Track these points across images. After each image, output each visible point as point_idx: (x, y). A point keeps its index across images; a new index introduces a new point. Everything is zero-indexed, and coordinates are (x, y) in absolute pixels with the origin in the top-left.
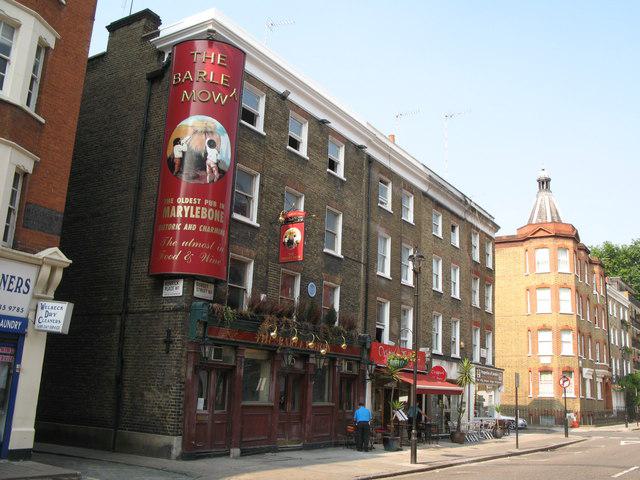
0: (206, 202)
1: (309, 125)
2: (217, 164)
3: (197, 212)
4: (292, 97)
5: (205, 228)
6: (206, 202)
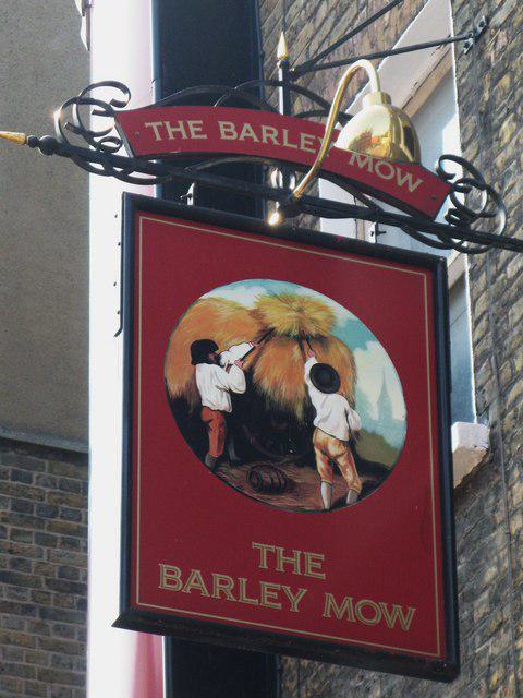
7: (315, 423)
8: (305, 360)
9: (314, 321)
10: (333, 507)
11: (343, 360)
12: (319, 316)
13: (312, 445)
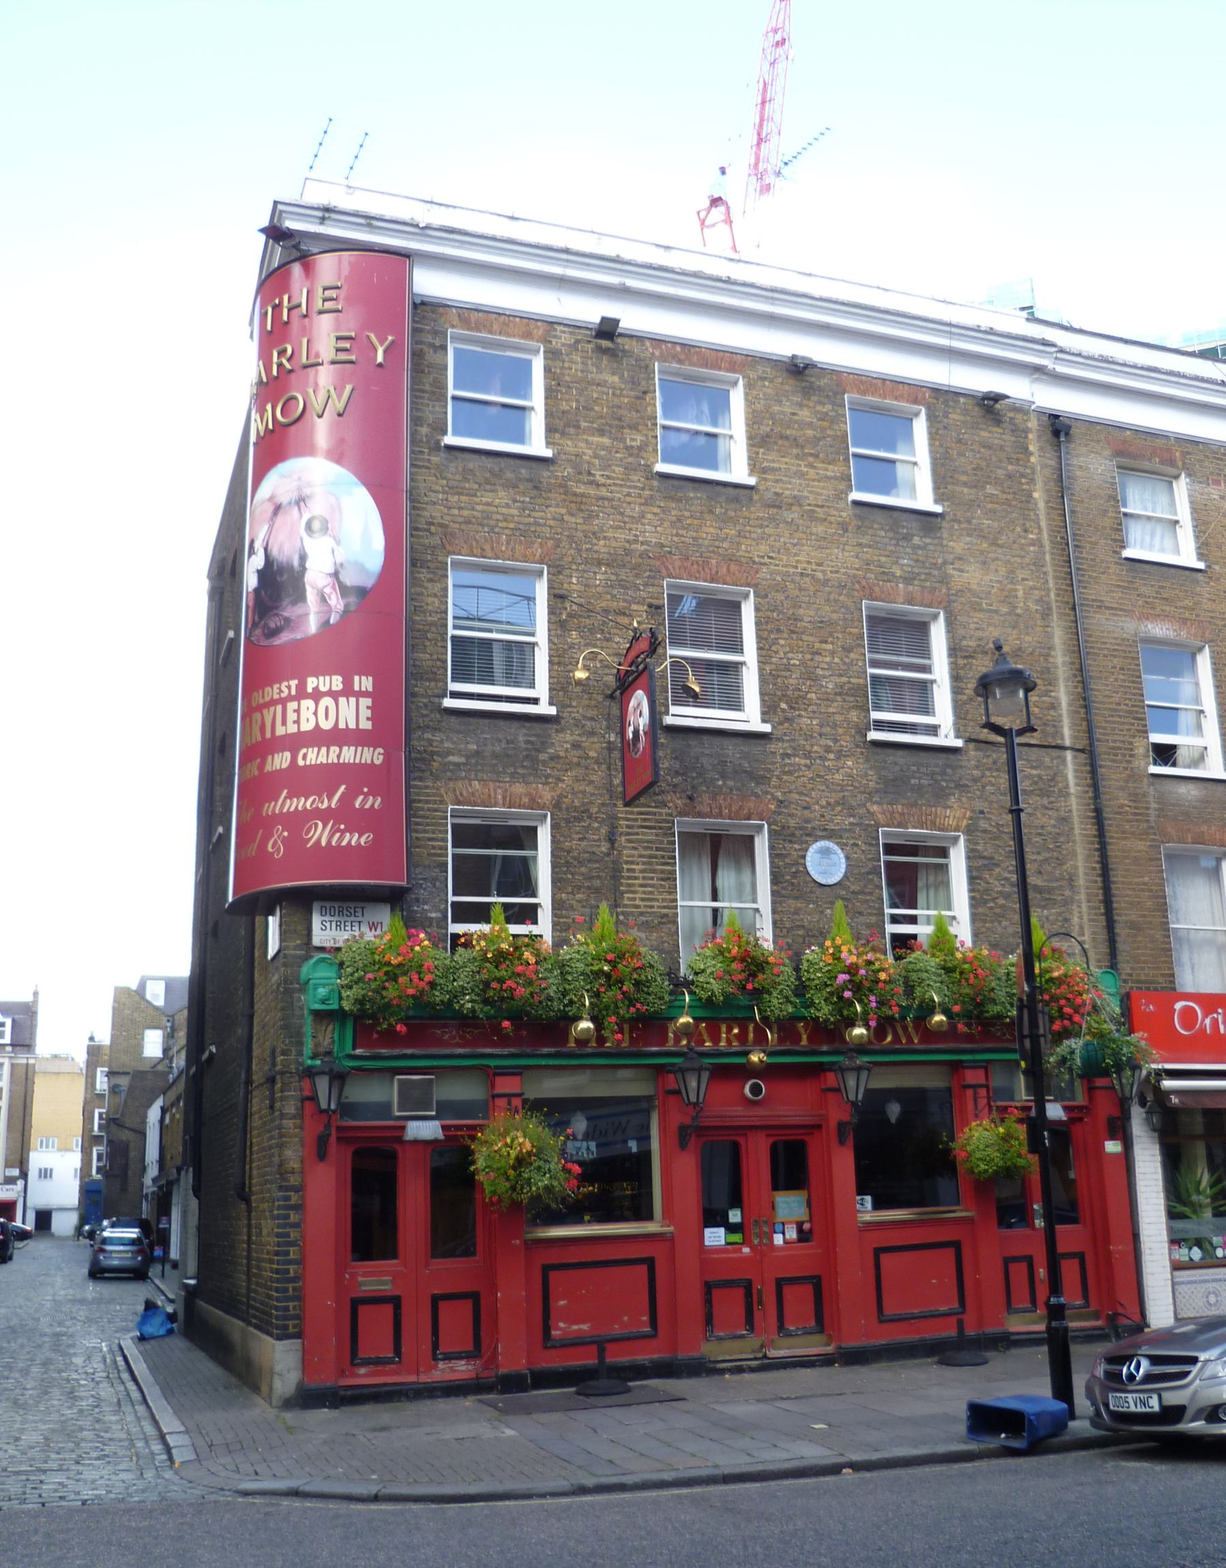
0: (311, 683)
1: (749, 386)
2: (336, 575)
3: (291, 716)
4: (633, 318)
6: (311, 683)
7: (308, 565)
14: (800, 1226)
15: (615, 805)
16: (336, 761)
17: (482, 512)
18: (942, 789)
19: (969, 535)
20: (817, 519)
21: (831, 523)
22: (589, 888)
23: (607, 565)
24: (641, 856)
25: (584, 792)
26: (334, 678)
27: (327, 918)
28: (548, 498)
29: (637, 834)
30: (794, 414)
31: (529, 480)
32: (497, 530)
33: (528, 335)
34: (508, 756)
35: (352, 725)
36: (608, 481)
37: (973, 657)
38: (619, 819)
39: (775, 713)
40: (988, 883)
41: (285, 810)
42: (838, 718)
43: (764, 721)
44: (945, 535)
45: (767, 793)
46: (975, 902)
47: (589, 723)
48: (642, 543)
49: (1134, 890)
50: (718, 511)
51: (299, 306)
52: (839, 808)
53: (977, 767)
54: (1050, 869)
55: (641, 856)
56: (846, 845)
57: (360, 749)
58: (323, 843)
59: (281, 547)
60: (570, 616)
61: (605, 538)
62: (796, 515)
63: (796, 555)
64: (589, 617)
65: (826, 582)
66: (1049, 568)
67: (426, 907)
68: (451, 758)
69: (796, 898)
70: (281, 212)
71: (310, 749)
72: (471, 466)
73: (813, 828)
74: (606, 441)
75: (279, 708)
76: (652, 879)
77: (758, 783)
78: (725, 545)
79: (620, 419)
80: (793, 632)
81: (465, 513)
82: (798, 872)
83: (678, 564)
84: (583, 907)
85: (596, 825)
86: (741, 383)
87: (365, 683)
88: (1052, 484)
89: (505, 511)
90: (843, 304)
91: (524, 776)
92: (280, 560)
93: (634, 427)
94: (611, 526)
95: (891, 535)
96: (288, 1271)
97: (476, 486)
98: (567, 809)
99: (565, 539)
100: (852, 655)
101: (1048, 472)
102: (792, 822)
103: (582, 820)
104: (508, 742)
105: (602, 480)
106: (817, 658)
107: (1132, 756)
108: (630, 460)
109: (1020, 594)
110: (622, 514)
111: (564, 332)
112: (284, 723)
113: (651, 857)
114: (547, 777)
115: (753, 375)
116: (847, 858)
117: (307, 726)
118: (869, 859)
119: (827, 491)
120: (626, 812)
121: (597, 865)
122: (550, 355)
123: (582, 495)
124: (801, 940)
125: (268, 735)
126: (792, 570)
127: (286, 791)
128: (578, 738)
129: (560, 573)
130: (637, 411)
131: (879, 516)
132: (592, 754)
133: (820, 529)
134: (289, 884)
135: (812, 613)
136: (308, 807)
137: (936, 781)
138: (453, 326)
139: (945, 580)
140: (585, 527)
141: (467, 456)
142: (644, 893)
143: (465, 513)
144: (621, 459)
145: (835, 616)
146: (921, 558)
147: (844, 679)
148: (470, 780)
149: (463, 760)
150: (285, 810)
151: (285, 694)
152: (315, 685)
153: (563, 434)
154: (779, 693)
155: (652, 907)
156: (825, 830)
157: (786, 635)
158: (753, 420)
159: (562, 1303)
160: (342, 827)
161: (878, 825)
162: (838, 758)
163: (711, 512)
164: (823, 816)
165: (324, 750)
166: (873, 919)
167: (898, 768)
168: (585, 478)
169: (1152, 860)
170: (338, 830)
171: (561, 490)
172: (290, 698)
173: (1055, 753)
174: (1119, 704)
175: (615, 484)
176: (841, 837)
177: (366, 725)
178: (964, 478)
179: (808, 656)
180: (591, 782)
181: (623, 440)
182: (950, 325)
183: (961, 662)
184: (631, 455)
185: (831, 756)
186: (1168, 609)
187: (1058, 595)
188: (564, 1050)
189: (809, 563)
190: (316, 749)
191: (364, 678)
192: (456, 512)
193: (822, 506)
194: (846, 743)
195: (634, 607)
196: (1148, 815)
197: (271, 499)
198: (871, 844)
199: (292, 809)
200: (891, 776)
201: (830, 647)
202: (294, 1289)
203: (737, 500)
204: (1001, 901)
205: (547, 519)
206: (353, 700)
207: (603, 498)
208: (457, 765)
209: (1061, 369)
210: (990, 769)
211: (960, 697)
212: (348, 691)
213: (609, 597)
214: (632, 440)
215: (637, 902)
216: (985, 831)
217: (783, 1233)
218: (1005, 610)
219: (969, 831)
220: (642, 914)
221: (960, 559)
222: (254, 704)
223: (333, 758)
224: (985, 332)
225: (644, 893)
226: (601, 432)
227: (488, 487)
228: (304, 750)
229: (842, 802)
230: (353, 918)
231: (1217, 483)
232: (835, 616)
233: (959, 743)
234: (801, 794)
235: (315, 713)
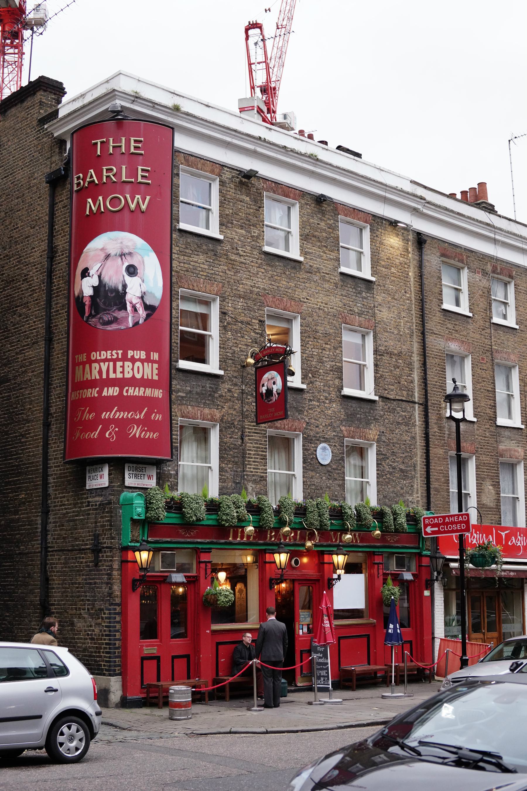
0: (130, 353)
1: (301, 208)
2: (142, 298)
3: (119, 369)
5: (131, 391)
6: (130, 353)
8: (123, 264)
9: (127, 247)
10: (133, 326)
11: (139, 261)
12: (130, 244)
13: (125, 300)
14: (308, 625)
15: (244, 421)
16: (143, 395)
17: (193, 266)
18: (369, 420)
19: (384, 293)
20: (326, 281)
21: (331, 283)
22: (233, 462)
23: (243, 298)
24: (254, 447)
25: (232, 414)
26: (142, 352)
27: (131, 472)
28: (220, 261)
29: (252, 436)
30: (318, 224)
31: (212, 251)
32: (199, 276)
33: (212, 172)
34: (203, 394)
35: (150, 378)
36: (245, 254)
37: (383, 355)
38: (245, 428)
39: (306, 379)
40: (384, 467)
41: (116, 417)
42: (331, 382)
43: (302, 383)
44: (375, 293)
45: (302, 418)
46: (379, 476)
47: (234, 379)
48: (257, 288)
49: (437, 472)
50: (287, 273)
51: (120, 147)
52: (329, 428)
53: (382, 410)
54: (407, 461)
55: (254, 447)
56: (332, 446)
57: (153, 389)
58: (137, 436)
59: (110, 278)
60: (228, 323)
61: (242, 284)
62: (317, 278)
63: (317, 298)
64: (235, 325)
65: (328, 314)
66: (413, 312)
67: (169, 468)
68: (180, 394)
69: (312, 471)
70: (115, 95)
71: (130, 388)
72: (189, 241)
73: (320, 437)
74: (243, 232)
75: (111, 364)
76: (257, 458)
77: (299, 414)
78: (290, 291)
79: (249, 221)
80: (315, 338)
81: (186, 266)
82: (313, 458)
83: (271, 299)
84: (231, 471)
85: (237, 431)
86: (298, 205)
87: (155, 356)
88: (417, 268)
89: (202, 266)
90: (344, 170)
91: (209, 404)
92: (110, 284)
93: (254, 225)
94: (245, 278)
95: (354, 291)
96: (115, 644)
97: (191, 252)
98: (226, 422)
99: (226, 282)
100: (337, 351)
101: (415, 262)
102: (312, 434)
103: (230, 427)
104: (202, 387)
105: (242, 253)
106: (324, 352)
107: (440, 408)
108: (253, 243)
109: (402, 324)
110: (249, 271)
111: (227, 171)
112: (115, 371)
113: (257, 448)
114: (218, 405)
115: (303, 202)
116: (332, 452)
117: (128, 376)
118: (340, 453)
119: (330, 265)
120: (249, 425)
121: (236, 451)
122: (221, 183)
123: (234, 261)
124: (313, 491)
125: (104, 376)
126: (316, 306)
127: (116, 408)
128: (230, 387)
129: (224, 301)
130: (256, 217)
131: (350, 281)
132: (236, 395)
133: (326, 286)
134: (120, 455)
135: (322, 329)
136: (129, 417)
137: (367, 416)
138: (182, 164)
139: (374, 315)
140: (235, 277)
141: (188, 235)
142: (254, 465)
143: (186, 266)
144: (249, 243)
145: (331, 331)
146: (366, 304)
147: (334, 363)
148: (188, 405)
149: (184, 395)
150: (116, 417)
151: (115, 357)
152: (132, 354)
153: (227, 227)
154: (308, 369)
155: (257, 472)
156: (324, 438)
157: (312, 340)
158: (302, 227)
159: (222, 660)
160: (146, 429)
161: (344, 437)
162: (330, 403)
163: (285, 273)
164: (323, 431)
165: (137, 389)
166: (341, 482)
167: (352, 409)
168: (235, 251)
169: (445, 459)
170: (144, 430)
171: (225, 257)
172: (117, 359)
173: (411, 405)
174: (436, 382)
175: (247, 256)
176: (330, 442)
177: (156, 378)
178: (383, 263)
179: (320, 351)
180: (235, 409)
181: (250, 232)
182: (386, 185)
183: (378, 357)
184: (253, 241)
185: (327, 401)
186: (457, 335)
187: (416, 326)
188: (228, 541)
189: (322, 303)
190: (133, 388)
191: (155, 353)
192: (182, 265)
193: (328, 274)
194: (333, 395)
195: (254, 321)
196: (444, 437)
197: (102, 249)
198: (341, 446)
199: (120, 417)
200: (350, 413)
201: (329, 346)
202: (118, 652)
203: (294, 268)
204: (388, 476)
205: (219, 272)
206: (150, 364)
207: (242, 263)
208: (182, 397)
209: (425, 211)
210: (387, 411)
211: (377, 375)
212: (148, 360)
213: (243, 315)
214: (254, 232)
215: (252, 470)
216: (384, 442)
217: (302, 629)
218: (396, 332)
219: (378, 441)
220: (253, 475)
221: (380, 305)
222: (93, 359)
223: (141, 394)
224: (399, 190)
225: (254, 465)
226: (242, 227)
227: (196, 253)
228: (127, 388)
229: (331, 425)
230: (141, 473)
231: (479, 273)
232: (331, 331)
233: (377, 398)
234: (315, 419)
235: (133, 369)
